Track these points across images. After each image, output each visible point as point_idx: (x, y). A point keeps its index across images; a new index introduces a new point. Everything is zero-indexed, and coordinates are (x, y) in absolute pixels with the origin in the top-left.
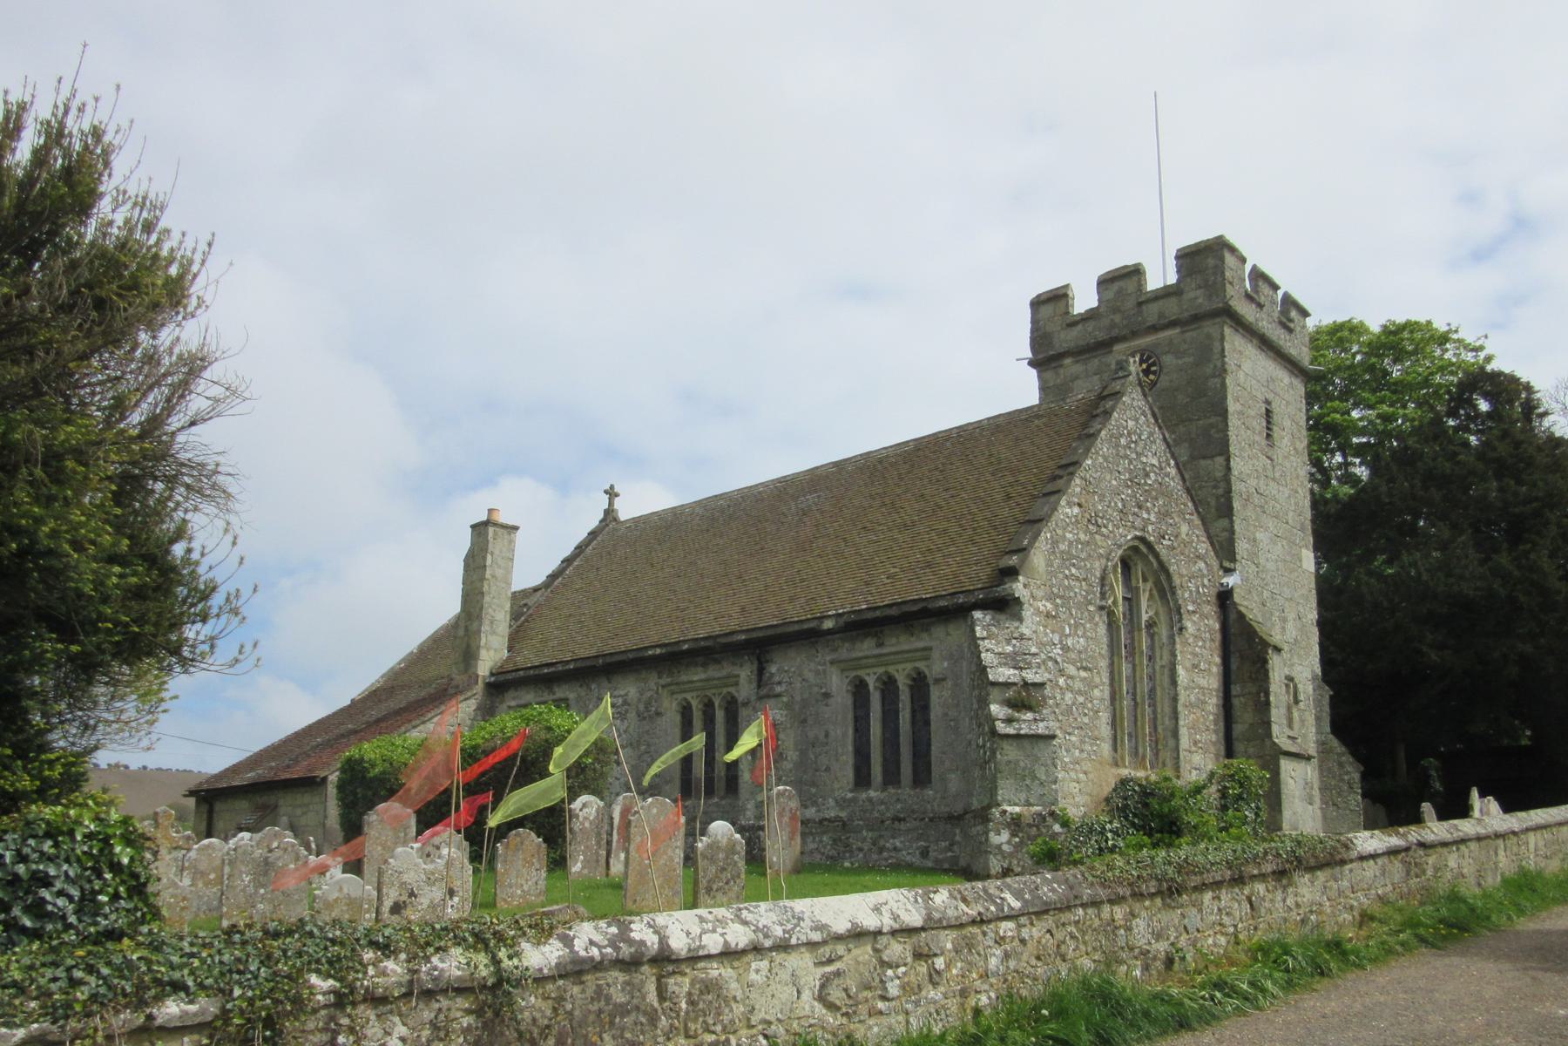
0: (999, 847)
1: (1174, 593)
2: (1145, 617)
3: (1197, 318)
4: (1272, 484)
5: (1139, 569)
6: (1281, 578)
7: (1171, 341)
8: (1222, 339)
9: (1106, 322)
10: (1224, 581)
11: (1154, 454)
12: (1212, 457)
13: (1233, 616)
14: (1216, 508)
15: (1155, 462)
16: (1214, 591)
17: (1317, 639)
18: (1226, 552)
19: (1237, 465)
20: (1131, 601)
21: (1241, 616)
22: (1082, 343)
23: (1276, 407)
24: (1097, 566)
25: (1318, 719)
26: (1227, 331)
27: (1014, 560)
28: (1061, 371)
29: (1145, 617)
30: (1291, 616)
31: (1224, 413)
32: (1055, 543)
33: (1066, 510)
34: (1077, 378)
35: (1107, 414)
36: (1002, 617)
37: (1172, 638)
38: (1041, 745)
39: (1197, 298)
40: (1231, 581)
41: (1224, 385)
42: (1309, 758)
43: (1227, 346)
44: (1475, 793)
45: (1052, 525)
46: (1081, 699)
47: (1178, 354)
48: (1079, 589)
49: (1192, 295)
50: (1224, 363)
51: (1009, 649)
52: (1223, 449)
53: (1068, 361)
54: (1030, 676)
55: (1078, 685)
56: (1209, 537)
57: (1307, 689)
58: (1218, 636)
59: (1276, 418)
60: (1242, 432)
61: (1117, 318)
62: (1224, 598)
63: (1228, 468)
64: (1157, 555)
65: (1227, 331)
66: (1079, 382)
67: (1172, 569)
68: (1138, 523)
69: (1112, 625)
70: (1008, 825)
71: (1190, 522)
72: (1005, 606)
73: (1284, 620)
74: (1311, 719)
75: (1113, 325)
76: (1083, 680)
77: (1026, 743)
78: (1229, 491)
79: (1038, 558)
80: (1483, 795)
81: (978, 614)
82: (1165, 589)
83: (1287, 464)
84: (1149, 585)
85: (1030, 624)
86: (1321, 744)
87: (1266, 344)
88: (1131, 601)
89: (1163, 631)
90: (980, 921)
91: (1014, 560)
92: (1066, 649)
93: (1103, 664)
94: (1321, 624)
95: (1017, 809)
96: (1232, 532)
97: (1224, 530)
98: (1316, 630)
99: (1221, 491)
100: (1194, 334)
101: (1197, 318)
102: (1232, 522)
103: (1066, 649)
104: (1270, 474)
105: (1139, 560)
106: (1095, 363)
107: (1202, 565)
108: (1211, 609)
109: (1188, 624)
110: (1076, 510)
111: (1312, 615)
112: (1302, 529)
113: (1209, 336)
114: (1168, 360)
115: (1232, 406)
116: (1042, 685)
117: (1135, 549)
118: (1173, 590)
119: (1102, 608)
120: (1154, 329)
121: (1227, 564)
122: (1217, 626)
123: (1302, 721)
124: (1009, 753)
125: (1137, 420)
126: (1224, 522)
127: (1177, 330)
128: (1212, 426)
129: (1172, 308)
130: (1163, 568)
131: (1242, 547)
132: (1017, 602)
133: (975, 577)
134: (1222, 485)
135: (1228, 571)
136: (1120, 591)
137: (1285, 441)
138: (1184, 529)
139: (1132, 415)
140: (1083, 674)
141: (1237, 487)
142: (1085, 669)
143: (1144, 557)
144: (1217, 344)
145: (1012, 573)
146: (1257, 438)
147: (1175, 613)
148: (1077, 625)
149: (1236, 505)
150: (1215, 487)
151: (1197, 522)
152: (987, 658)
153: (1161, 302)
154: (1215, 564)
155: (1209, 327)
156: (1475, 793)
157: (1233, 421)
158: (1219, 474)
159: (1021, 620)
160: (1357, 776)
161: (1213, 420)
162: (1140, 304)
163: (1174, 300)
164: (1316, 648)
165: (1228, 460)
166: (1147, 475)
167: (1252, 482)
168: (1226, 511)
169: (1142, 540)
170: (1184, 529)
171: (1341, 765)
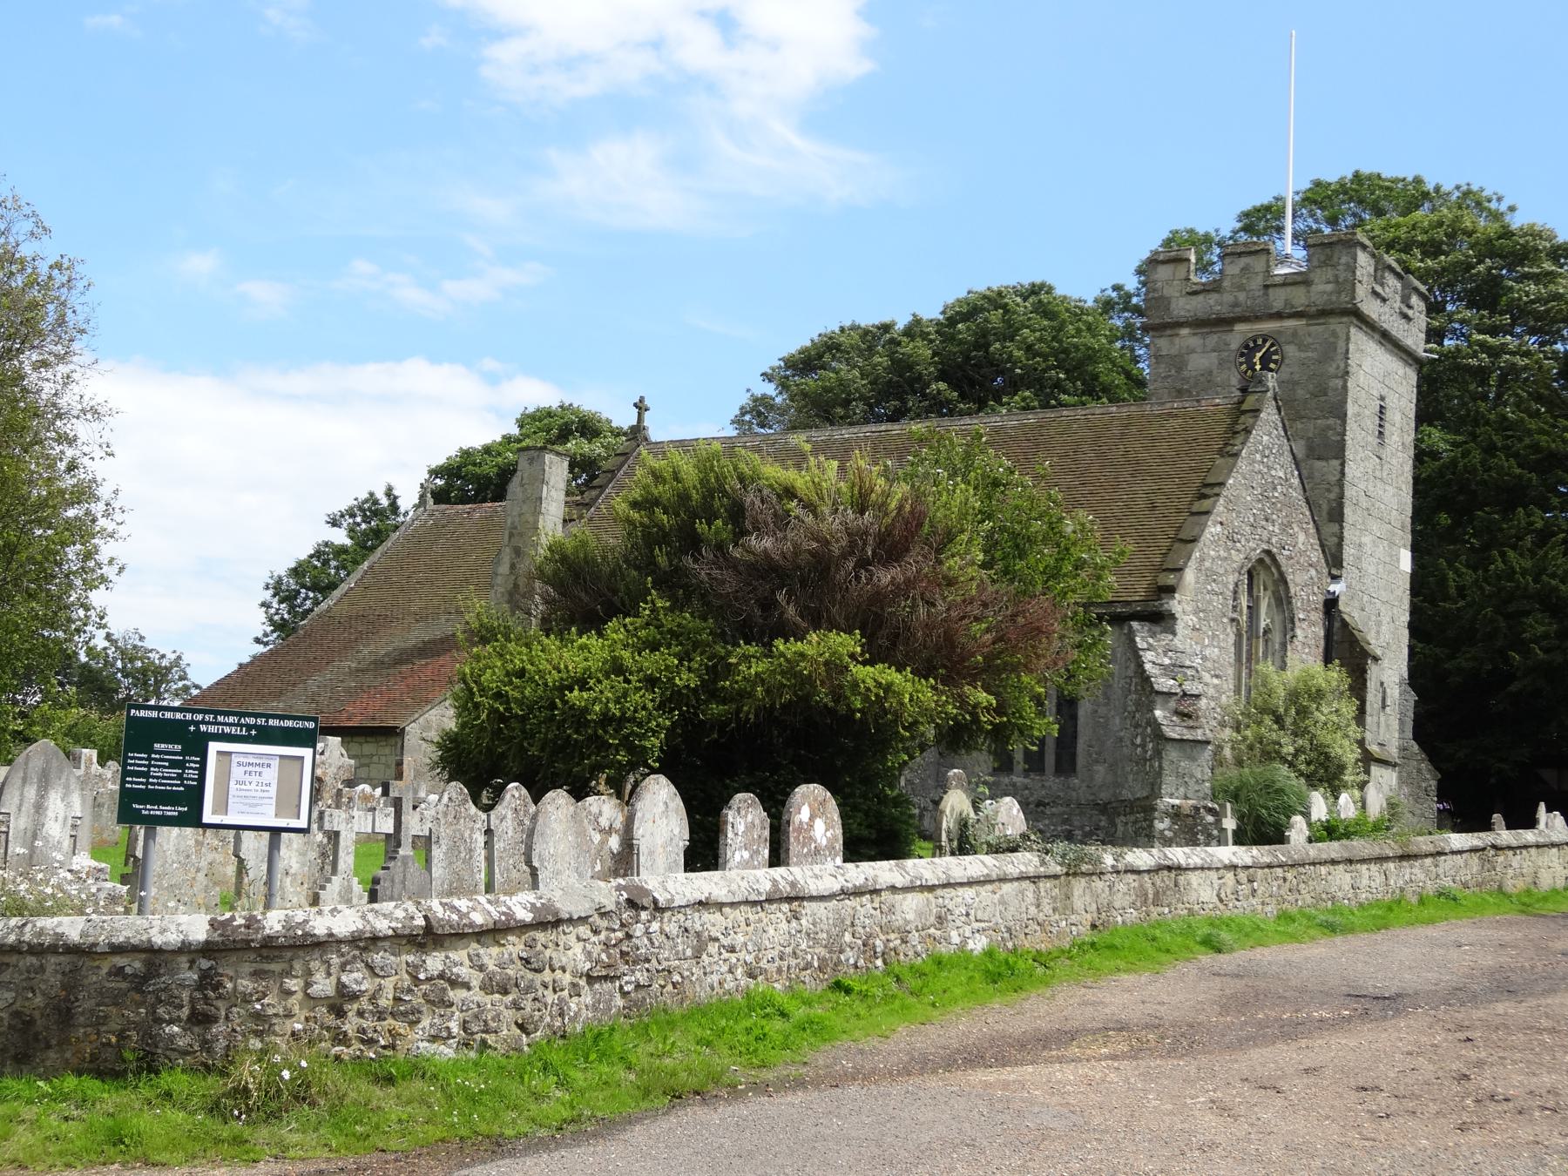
0: (1162, 832)
1: (1290, 603)
2: (1263, 625)
3: (1324, 313)
4: (1379, 483)
5: (1262, 576)
6: (1379, 581)
7: (1295, 333)
8: (1348, 339)
9: (1228, 298)
10: (1332, 588)
11: (1283, 470)
12: (1327, 459)
13: (1337, 624)
14: (1329, 513)
15: (1281, 474)
16: (1321, 598)
17: (1407, 641)
18: (1334, 561)
19: (1351, 470)
20: (1253, 610)
21: (1345, 624)
22: (1200, 315)
23: (1389, 403)
24: (1232, 579)
25: (1402, 722)
26: (1353, 330)
27: (1171, 579)
28: (1177, 340)
29: (1263, 625)
30: (1386, 619)
31: (1343, 417)
32: (1202, 560)
33: (1212, 530)
34: (1193, 351)
35: (1248, 431)
36: (1157, 629)
37: (1284, 646)
38: (1199, 747)
39: (1322, 289)
40: (1336, 588)
41: (1345, 387)
42: (1395, 765)
43: (1352, 347)
44: (1542, 807)
45: (1200, 545)
46: (1213, 704)
47: (1302, 347)
48: (1217, 602)
49: (1321, 287)
50: (1347, 365)
51: (1167, 661)
52: (1338, 451)
53: (1185, 331)
54: (1190, 687)
55: (1211, 692)
56: (1322, 546)
57: (1394, 692)
58: (1322, 642)
59: (1388, 415)
60: (1358, 435)
61: (1242, 296)
62: (1331, 604)
63: (1343, 473)
64: (1278, 566)
65: (1353, 330)
66: (1194, 356)
67: (1289, 578)
68: (1265, 535)
69: (1239, 635)
70: (1167, 814)
71: (1306, 531)
72: (1161, 619)
73: (1379, 624)
74: (1395, 725)
75: (1236, 304)
76: (1215, 686)
77: (1187, 747)
78: (1342, 496)
79: (1190, 575)
80: (1549, 810)
81: (1135, 624)
82: (1283, 600)
83: (1394, 461)
84: (1269, 593)
85: (1183, 637)
86: (1403, 749)
87: (1386, 338)
88: (1253, 610)
89: (1276, 637)
90: (1270, 866)
91: (1171, 579)
92: (1204, 658)
93: (1231, 671)
94: (1412, 627)
95: (1177, 802)
96: (1341, 538)
97: (1334, 535)
98: (1406, 632)
99: (1332, 496)
100: (1320, 329)
101: (1324, 313)
102: (1342, 528)
103: (1204, 658)
104: (1378, 474)
105: (1265, 572)
106: (1213, 340)
107: (1313, 572)
108: (1317, 616)
109: (1299, 632)
110: (1219, 528)
111: (1406, 618)
112: (1403, 528)
113: (1334, 334)
114: (1291, 351)
115: (1351, 409)
116: (1198, 696)
117: (1260, 561)
118: (1289, 599)
119: (1233, 620)
120: (1279, 316)
121: (1334, 572)
122: (1322, 633)
123: (1388, 726)
124: (1172, 754)
125: (1270, 435)
126: (1335, 528)
127: (1304, 322)
128: (1329, 427)
129: (1299, 298)
130: (1283, 580)
131: (1349, 553)
132: (1173, 617)
133: (1138, 591)
134: (1336, 489)
135: (1335, 578)
136: (1244, 601)
137: (1395, 438)
138: (1302, 537)
139: (1267, 431)
140: (1216, 681)
141: (1349, 492)
142: (1217, 676)
143: (1268, 568)
144: (1341, 344)
145: (1171, 590)
146: (1370, 439)
147: (1289, 623)
148: (1214, 636)
149: (1347, 511)
150: (1329, 490)
151: (1312, 531)
152: (1148, 666)
153: (1289, 289)
154: (1325, 571)
155: (1335, 324)
156: (1542, 807)
157: (1351, 425)
158: (1334, 479)
159: (1174, 633)
160: (1434, 783)
161: (1331, 421)
162: (1266, 287)
163: (1301, 290)
164: (1406, 651)
165: (1343, 465)
166: (1275, 489)
167: (1362, 486)
168: (1337, 515)
169: (1268, 552)
170: (1302, 537)
171: (1419, 771)
